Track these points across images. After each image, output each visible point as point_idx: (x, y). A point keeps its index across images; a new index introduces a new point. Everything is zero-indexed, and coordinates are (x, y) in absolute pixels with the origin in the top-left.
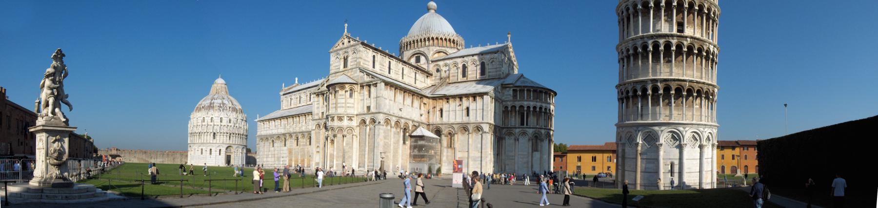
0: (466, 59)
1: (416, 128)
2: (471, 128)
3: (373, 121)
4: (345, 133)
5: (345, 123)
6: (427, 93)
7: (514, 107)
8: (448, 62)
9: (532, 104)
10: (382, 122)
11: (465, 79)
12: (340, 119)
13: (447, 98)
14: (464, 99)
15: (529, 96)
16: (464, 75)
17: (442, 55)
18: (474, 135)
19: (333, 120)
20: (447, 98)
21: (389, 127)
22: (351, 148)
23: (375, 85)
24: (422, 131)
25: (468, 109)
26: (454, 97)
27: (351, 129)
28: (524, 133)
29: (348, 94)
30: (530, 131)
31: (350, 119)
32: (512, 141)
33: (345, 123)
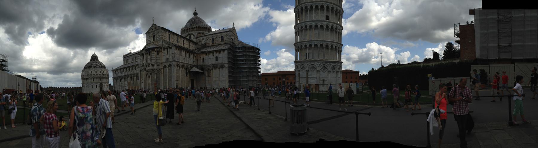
1: (191, 68)
2: (219, 66)
3: (170, 66)
5: (156, 67)
6: (196, 51)
10: (175, 65)
12: (153, 65)
13: (206, 53)
17: (202, 35)
18: (221, 69)
19: (149, 66)
20: (206, 53)
24: (195, 69)
25: (217, 57)
26: (210, 52)
29: (156, 53)
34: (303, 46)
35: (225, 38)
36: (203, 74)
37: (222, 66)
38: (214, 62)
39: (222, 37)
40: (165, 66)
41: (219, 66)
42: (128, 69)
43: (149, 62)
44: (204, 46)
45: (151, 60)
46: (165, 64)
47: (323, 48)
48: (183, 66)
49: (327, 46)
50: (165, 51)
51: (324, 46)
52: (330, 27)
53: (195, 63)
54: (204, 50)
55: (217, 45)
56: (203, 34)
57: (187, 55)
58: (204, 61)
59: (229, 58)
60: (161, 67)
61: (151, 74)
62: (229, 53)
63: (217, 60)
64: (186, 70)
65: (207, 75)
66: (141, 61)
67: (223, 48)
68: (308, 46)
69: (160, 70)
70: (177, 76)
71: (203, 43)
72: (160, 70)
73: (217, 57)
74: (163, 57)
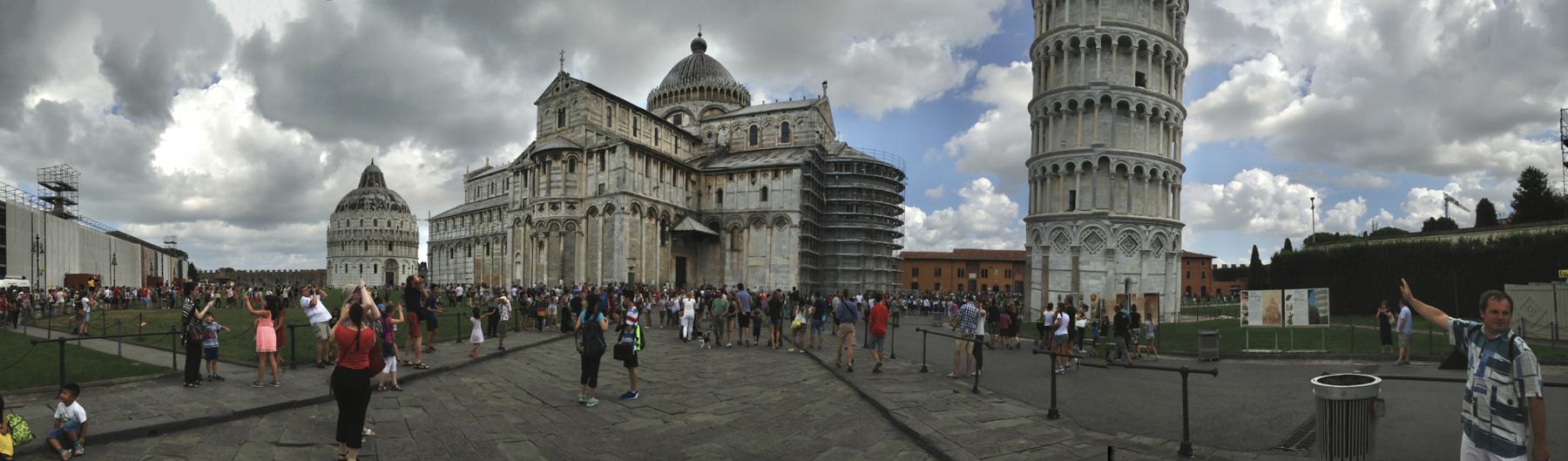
0: (758, 118)
1: (680, 218)
2: (769, 219)
3: (610, 209)
4: (563, 230)
5: (563, 212)
6: (696, 166)
8: (728, 122)
10: (627, 208)
11: (756, 147)
12: (554, 207)
14: (759, 176)
16: (753, 141)
18: (775, 230)
19: (541, 209)
20: (730, 174)
21: (638, 217)
22: (573, 254)
23: (613, 150)
24: (690, 224)
25: (764, 190)
26: (741, 171)
27: (571, 223)
31: (571, 206)
34: (1062, 168)
35: (794, 131)
36: (715, 240)
38: (754, 203)
39: (785, 125)
40: (593, 211)
41: (769, 219)
43: (543, 194)
44: (725, 152)
45: (549, 189)
46: (595, 203)
47: (1126, 178)
48: (652, 213)
49: (1139, 170)
50: (595, 161)
51: (1131, 170)
52: (1149, 111)
53: (692, 205)
54: (722, 164)
55: (767, 152)
56: (723, 111)
58: (720, 200)
59: (804, 194)
60: (580, 212)
61: (547, 235)
62: (805, 180)
63: (764, 197)
64: (663, 226)
65: (728, 245)
66: (518, 192)
67: (789, 161)
68: (1078, 167)
69: (577, 221)
70: (632, 245)
71: (722, 142)
72: (577, 221)
73: (764, 190)
74: (589, 178)
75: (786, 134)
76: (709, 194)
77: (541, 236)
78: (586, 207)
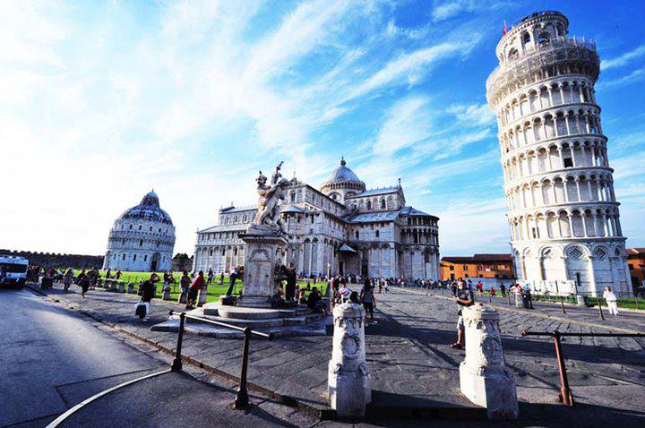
1: (341, 245)
3: (315, 240)
5: (294, 240)
7: (409, 230)
8: (358, 200)
9: (423, 228)
13: (362, 224)
15: (420, 221)
18: (383, 250)
20: (362, 224)
24: (346, 248)
25: (377, 232)
26: (367, 224)
27: (299, 245)
28: (418, 249)
29: (296, 220)
30: (423, 247)
32: (408, 255)
33: (294, 240)
37: (386, 246)
38: (372, 238)
39: (383, 201)
40: (307, 240)
42: (231, 235)
46: (308, 237)
54: (357, 220)
56: (355, 194)
57: (337, 225)
58: (357, 236)
60: (301, 241)
63: (377, 235)
67: (388, 219)
75: (383, 206)
76: (353, 234)
77: (284, 250)
78: (305, 238)
